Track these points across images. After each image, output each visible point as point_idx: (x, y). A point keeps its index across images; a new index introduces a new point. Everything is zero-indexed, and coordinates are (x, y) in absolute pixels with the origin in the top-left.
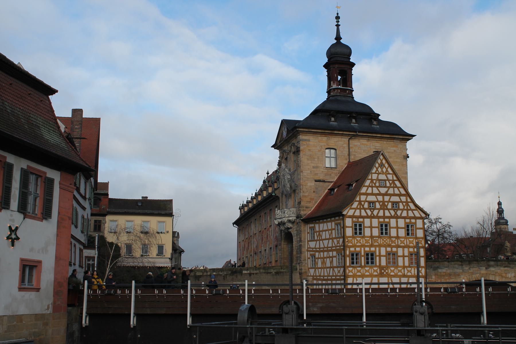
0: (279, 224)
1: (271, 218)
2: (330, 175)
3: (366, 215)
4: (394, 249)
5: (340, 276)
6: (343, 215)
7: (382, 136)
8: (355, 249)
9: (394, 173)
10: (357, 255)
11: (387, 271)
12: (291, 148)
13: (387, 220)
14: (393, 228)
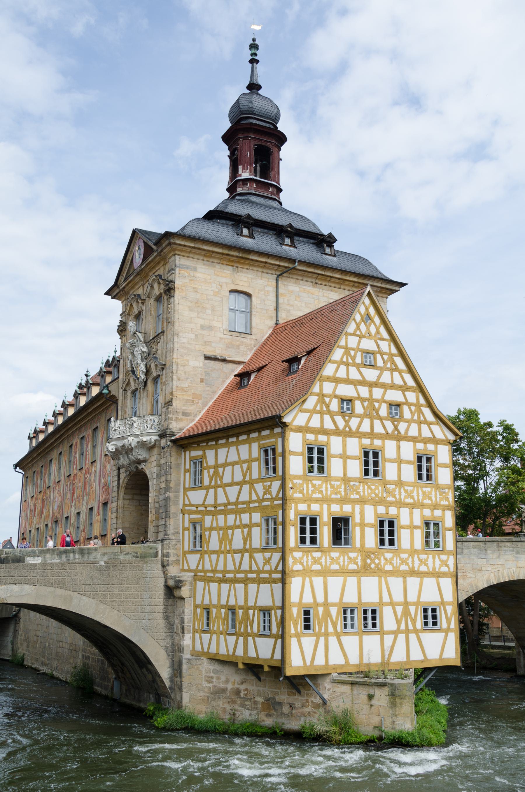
0: (116, 455)
1: (94, 447)
2: (238, 347)
3: (333, 427)
4: (393, 511)
5: (270, 572)
6: (284, 425)
7: (344, 277)
8: (309, 506)
9: (393, 339)
10: (313, 521)
11: (377, 561)
12: (152, 287)
13: (377, 443)
14: (391, 461)
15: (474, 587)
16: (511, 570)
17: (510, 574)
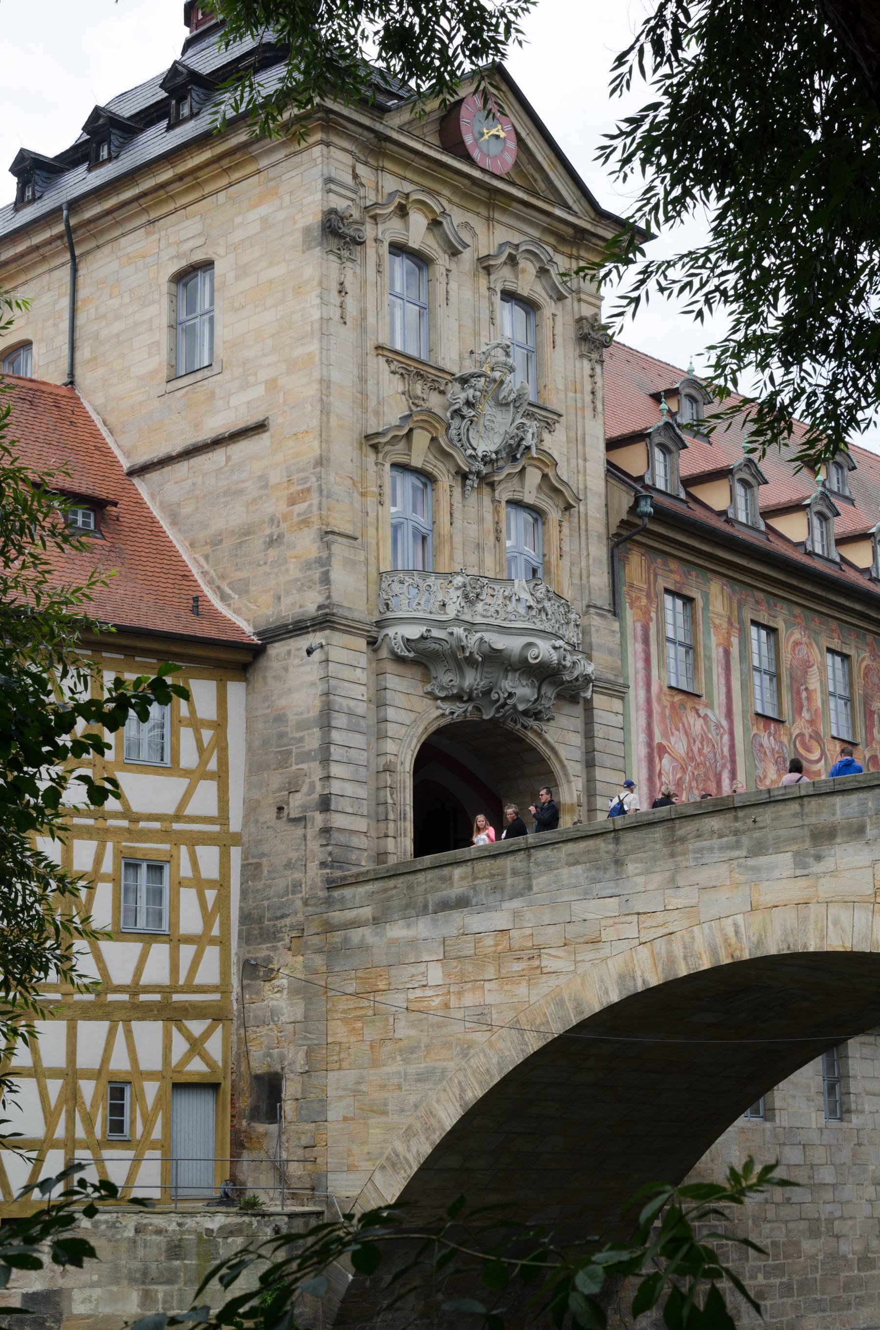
15: (570, 1005)
16: (728, 923)
17: (719, 941)
